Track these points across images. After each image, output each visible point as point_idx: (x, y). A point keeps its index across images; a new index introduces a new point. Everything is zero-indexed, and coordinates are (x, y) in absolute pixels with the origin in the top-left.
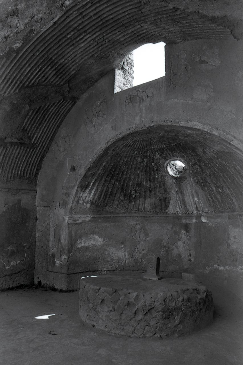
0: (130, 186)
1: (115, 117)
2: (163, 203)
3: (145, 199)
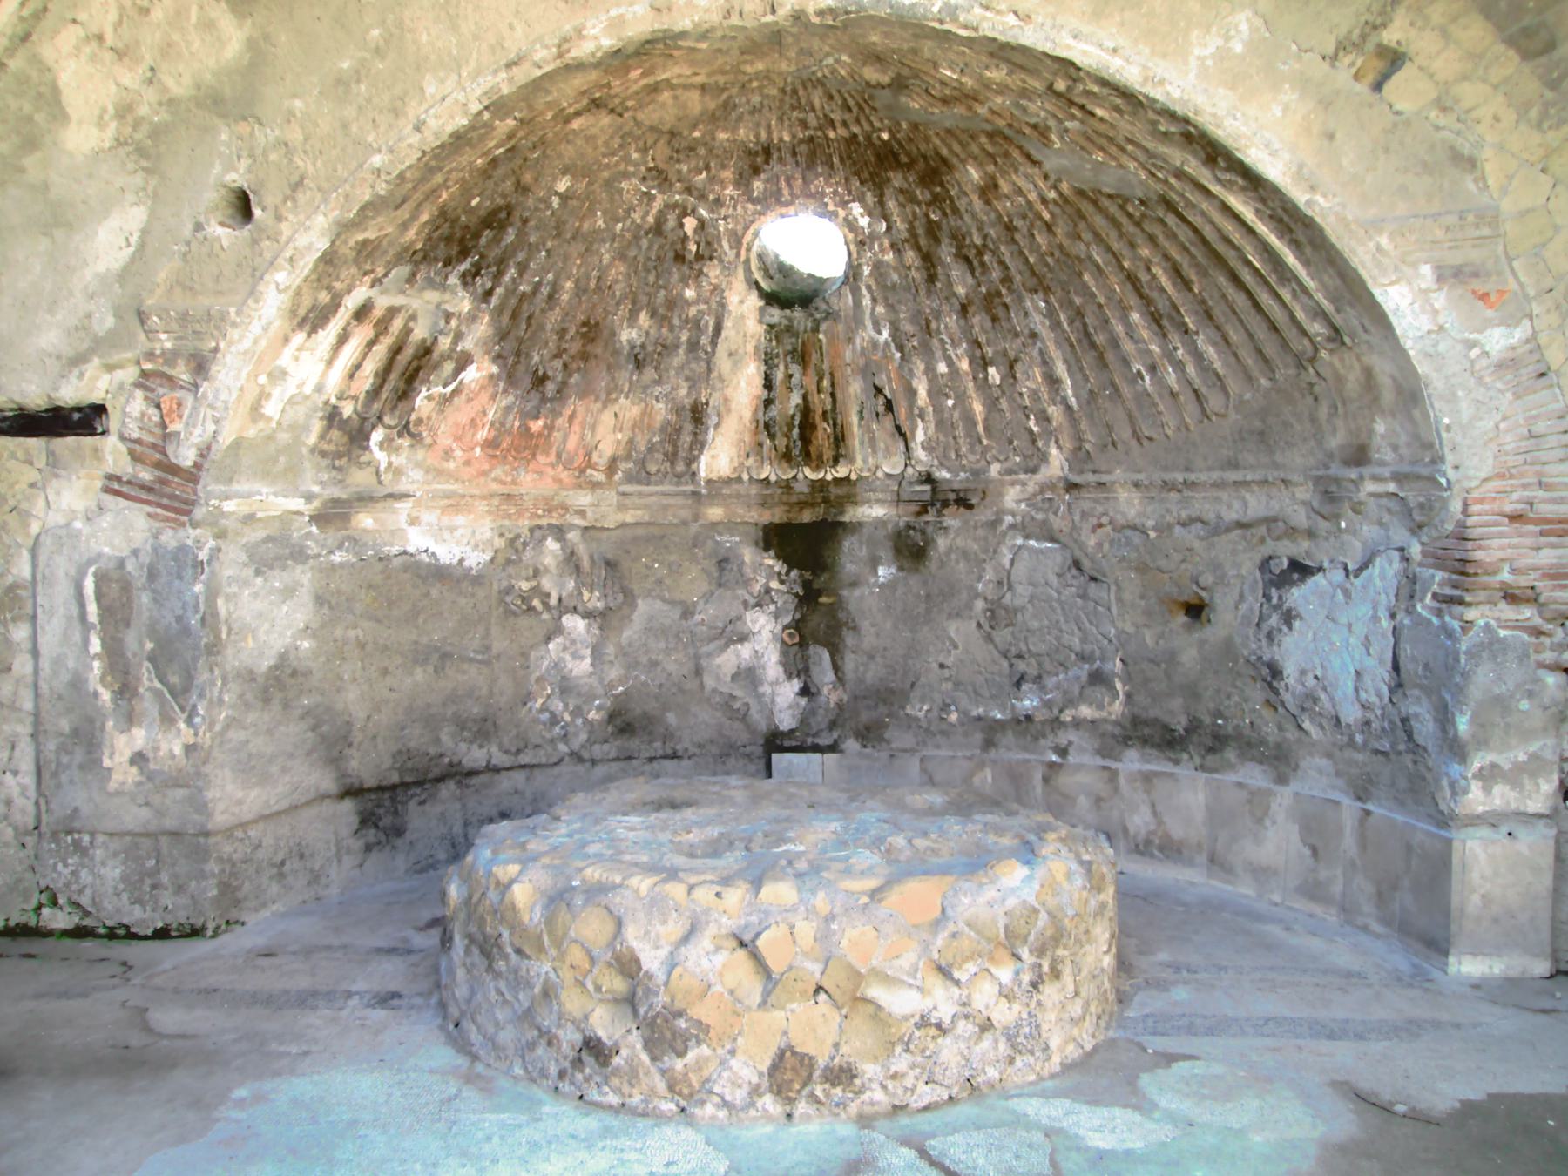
2: (689, 427)
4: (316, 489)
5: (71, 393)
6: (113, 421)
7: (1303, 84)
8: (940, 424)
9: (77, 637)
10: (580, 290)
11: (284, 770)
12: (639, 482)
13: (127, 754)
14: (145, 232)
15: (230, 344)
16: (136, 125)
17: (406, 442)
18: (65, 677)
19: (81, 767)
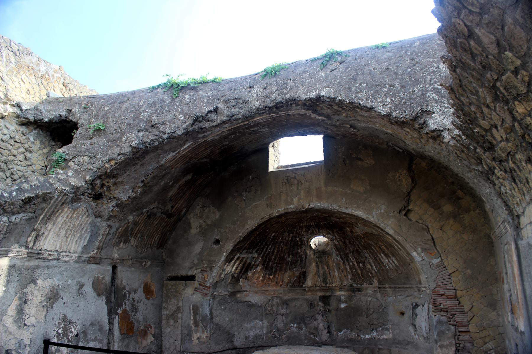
1: (270, 195)
2: (302, 276)
3: (285, 271)
4: (230, 290)
5: (190, 273)
6: (196, 278)
8: (353, 275)
10: (278, 252)
11: (223, 343)
14: (203, 246)
15: (216, 265)
17: (246, 281)
19: (188, 340)
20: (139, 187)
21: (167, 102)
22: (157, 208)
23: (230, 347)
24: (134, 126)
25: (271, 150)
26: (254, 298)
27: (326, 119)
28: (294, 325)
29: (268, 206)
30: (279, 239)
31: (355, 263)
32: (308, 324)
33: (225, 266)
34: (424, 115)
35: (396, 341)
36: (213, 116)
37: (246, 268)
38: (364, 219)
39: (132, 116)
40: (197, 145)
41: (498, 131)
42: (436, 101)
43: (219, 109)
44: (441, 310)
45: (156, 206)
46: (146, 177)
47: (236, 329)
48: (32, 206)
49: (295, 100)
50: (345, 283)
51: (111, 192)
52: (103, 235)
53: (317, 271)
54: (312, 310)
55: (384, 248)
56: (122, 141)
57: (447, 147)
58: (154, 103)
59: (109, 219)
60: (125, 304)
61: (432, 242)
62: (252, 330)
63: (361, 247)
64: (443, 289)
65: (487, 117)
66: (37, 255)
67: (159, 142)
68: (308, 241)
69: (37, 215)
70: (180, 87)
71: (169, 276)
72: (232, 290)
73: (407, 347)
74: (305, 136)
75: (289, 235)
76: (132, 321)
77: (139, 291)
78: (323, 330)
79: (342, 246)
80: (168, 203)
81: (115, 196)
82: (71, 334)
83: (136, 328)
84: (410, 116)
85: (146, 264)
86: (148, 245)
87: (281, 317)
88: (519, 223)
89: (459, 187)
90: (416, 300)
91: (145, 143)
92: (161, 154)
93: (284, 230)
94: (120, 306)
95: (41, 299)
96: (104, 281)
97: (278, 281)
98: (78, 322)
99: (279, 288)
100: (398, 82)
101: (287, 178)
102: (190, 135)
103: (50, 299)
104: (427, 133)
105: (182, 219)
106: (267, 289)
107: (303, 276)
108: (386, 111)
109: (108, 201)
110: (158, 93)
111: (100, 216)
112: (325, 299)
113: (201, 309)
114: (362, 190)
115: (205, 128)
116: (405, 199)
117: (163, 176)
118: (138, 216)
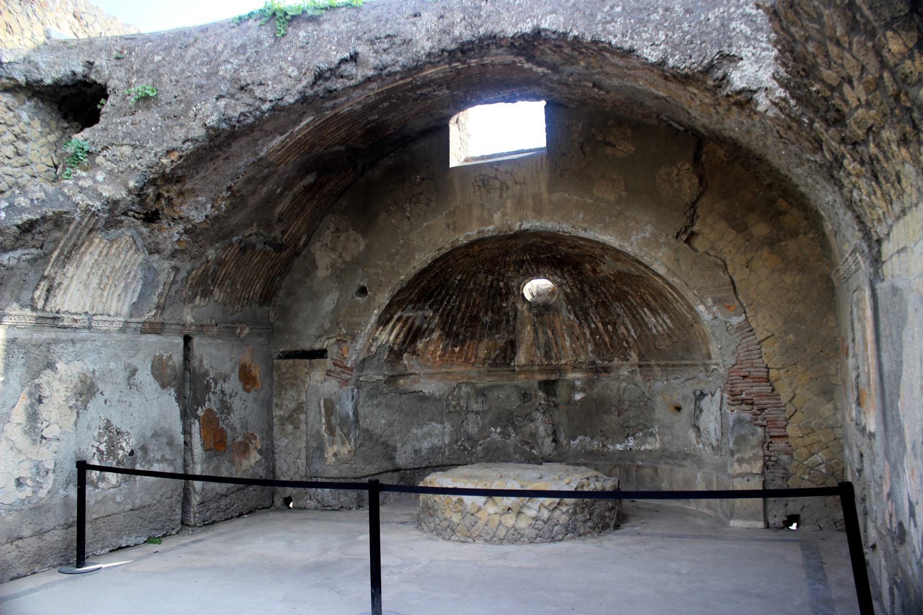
0: (456, 319)
2: (509, 348)
3: (480, 340)
4: (386, 373)
5: (317, 346)
6: (329, 354)
7: (667, 244)
8: (596, 344)
9: (318, 418)
10: (467, 306)
11: (377, 461)
12: (494, 367)
13: (332, 454)
14: (338, 299)
15: (362, 331)
16: (336, 270)
17: (414, 357)
18: (315, 430)
20: (223, 199)
21: (267, 44)
22: (256, 234)
23: (390, 467)
24: (210, 89)
25: (453, 128)
26: (428, 386)
27: (550, 72)
28: (496, 430)
29: (449, 228)
30: (469, 283)
31: (600, 325)
32: (519, 427)
33: (378, 333)
34: (725, 62)
35: (666, 453)
36: (349, 68)
37: (413, 335)
38: (614, 248)
39: (205, 70)
40: (322, 120)
41: (853, 88)
42: (747, 38)
43: (360, 55)
44: (743, 401)
45: (254, 231)
46: (235, 181)
47: (398, 437)
48: (37, 237)
49: (495, 37)
50: (582, 358)
51: (175, 208)
52: (165, 284)
53: (534, 339)
54: (525, 404)
55: (650, 299)
56: (188, 117)
57: (763, 121)
58: (244, 47)
59: (173, 255)
60: (209, 400)
61: (732, 287)
62: (426, 439)
63: (610, 297)
64: (747, 367)
65: (835, 63)
66: (54, 320)
67: (255, 117)
68: (520, 288)
69: (47, 251)
70: (288, 17)
71: (282, 352)
72: (390, 374)
73: (684, 463)
74: (514, 102)
75: (487, 277)
76: (222, 428)
77: (232, 378)
78: (545, 437)
79: (577, 295)
80: (276, 226)
81: (182, 214)
82: (121, 452)
83: (229, 440)
84: (700, 65)
85: (241, 332)
86: (244, 299)
87: (474, 416)
88: (879, 252)
89: (781, 193)
90: (702, 386)
91: (230, 119)
92: (259, 139)
93: (478, 268)
94: (201, 403)
95: (65, 396)
96: (170, 363)
97: (469, 355)
98: (132, 432)
99: (469, 368)
100: (679, 4)
101: (482, 177)
102: (309, 103)
103: (81, 395)
104: (728, 96)
105: (300, 253)
106: (451, 370)
107: (512, 346)
108: (657, 56)
109: (169, 225)
110: (249, 28)
111: (158, 252)
112: (548, 387)
113: (338, 406)
114: (612, 197)
115: (335, 90)
116: (688, 214)
117: (266, 178)
118: (224, 249)
